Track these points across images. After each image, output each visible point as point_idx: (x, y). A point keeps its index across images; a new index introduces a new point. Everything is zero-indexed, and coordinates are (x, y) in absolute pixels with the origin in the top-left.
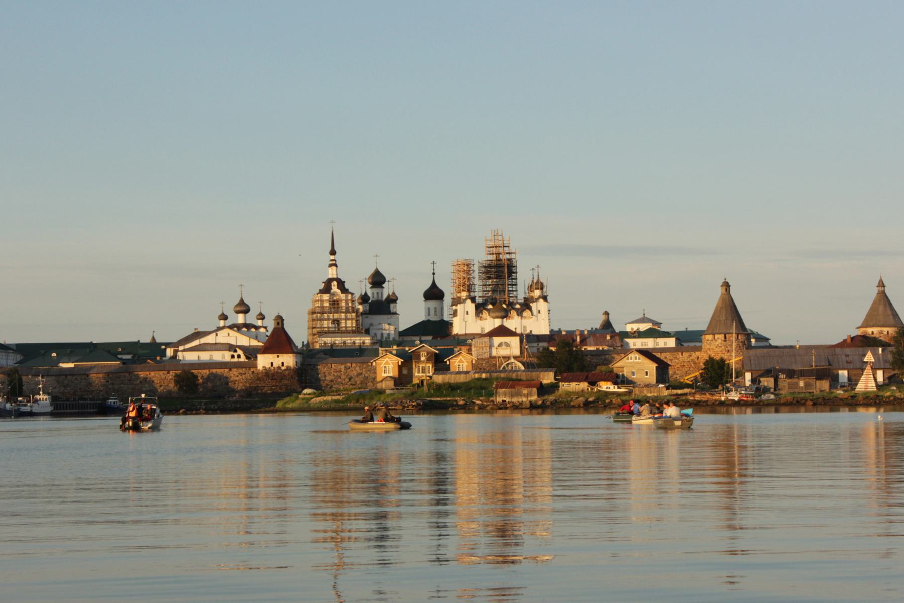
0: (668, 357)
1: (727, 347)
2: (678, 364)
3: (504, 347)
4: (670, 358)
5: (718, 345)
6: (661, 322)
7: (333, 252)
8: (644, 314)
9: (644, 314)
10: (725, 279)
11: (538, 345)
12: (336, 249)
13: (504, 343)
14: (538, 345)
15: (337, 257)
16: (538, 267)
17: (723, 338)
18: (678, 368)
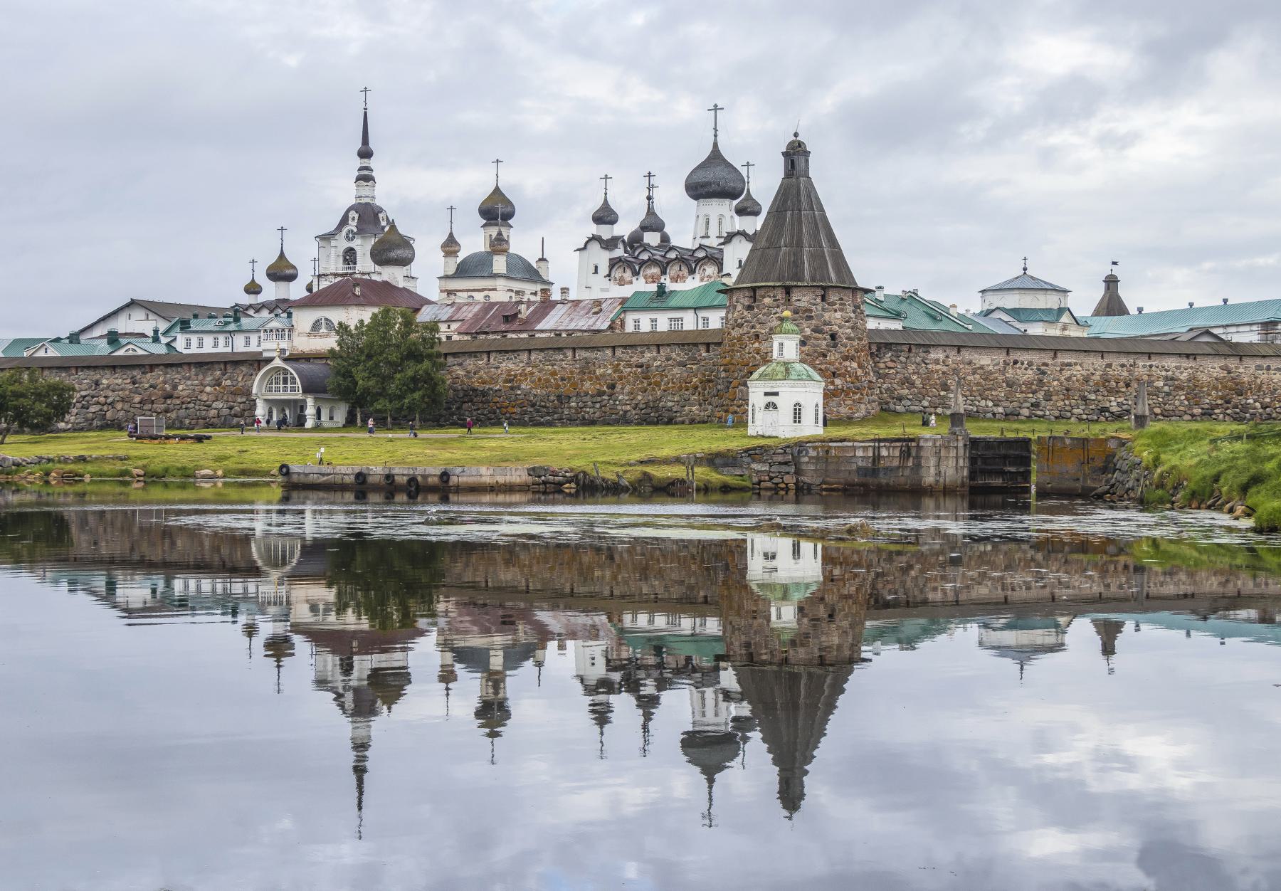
0: (674, 355)
1: (753, 327)
2: (695, 376)
3: (323, 330)
4: (679, 359)
5: (736, 321)
6: (1068, 288)
7: (365, 153)
8: (1025, 269)
9: (1025, 269)
10: (796, 135)
11: (449, 327)
12: (371, 145)
13: (323, 321)
14: (449, 327)
15: (372, 163)
16: (748, 164)
17: (747, 302)
18: (696, 388)
